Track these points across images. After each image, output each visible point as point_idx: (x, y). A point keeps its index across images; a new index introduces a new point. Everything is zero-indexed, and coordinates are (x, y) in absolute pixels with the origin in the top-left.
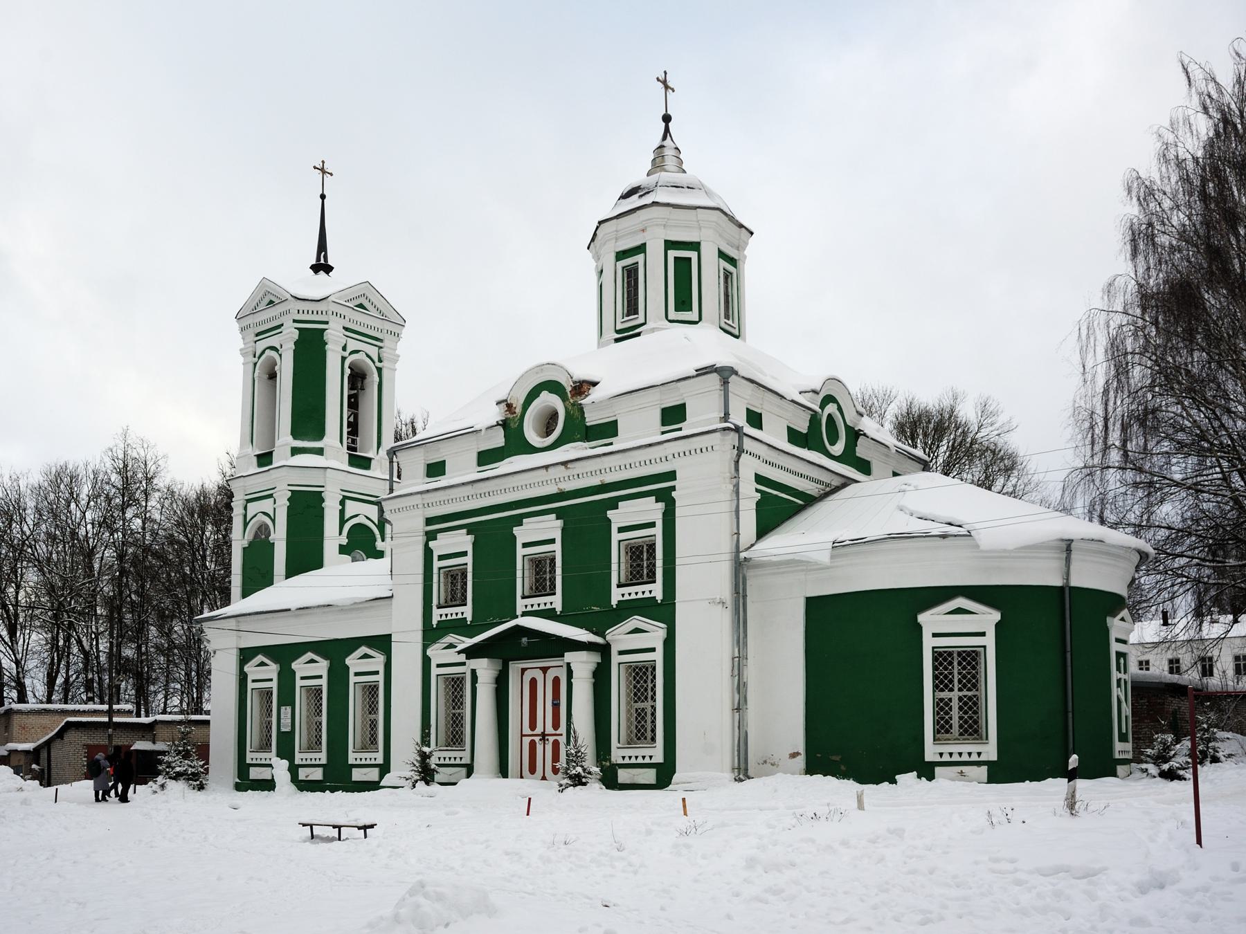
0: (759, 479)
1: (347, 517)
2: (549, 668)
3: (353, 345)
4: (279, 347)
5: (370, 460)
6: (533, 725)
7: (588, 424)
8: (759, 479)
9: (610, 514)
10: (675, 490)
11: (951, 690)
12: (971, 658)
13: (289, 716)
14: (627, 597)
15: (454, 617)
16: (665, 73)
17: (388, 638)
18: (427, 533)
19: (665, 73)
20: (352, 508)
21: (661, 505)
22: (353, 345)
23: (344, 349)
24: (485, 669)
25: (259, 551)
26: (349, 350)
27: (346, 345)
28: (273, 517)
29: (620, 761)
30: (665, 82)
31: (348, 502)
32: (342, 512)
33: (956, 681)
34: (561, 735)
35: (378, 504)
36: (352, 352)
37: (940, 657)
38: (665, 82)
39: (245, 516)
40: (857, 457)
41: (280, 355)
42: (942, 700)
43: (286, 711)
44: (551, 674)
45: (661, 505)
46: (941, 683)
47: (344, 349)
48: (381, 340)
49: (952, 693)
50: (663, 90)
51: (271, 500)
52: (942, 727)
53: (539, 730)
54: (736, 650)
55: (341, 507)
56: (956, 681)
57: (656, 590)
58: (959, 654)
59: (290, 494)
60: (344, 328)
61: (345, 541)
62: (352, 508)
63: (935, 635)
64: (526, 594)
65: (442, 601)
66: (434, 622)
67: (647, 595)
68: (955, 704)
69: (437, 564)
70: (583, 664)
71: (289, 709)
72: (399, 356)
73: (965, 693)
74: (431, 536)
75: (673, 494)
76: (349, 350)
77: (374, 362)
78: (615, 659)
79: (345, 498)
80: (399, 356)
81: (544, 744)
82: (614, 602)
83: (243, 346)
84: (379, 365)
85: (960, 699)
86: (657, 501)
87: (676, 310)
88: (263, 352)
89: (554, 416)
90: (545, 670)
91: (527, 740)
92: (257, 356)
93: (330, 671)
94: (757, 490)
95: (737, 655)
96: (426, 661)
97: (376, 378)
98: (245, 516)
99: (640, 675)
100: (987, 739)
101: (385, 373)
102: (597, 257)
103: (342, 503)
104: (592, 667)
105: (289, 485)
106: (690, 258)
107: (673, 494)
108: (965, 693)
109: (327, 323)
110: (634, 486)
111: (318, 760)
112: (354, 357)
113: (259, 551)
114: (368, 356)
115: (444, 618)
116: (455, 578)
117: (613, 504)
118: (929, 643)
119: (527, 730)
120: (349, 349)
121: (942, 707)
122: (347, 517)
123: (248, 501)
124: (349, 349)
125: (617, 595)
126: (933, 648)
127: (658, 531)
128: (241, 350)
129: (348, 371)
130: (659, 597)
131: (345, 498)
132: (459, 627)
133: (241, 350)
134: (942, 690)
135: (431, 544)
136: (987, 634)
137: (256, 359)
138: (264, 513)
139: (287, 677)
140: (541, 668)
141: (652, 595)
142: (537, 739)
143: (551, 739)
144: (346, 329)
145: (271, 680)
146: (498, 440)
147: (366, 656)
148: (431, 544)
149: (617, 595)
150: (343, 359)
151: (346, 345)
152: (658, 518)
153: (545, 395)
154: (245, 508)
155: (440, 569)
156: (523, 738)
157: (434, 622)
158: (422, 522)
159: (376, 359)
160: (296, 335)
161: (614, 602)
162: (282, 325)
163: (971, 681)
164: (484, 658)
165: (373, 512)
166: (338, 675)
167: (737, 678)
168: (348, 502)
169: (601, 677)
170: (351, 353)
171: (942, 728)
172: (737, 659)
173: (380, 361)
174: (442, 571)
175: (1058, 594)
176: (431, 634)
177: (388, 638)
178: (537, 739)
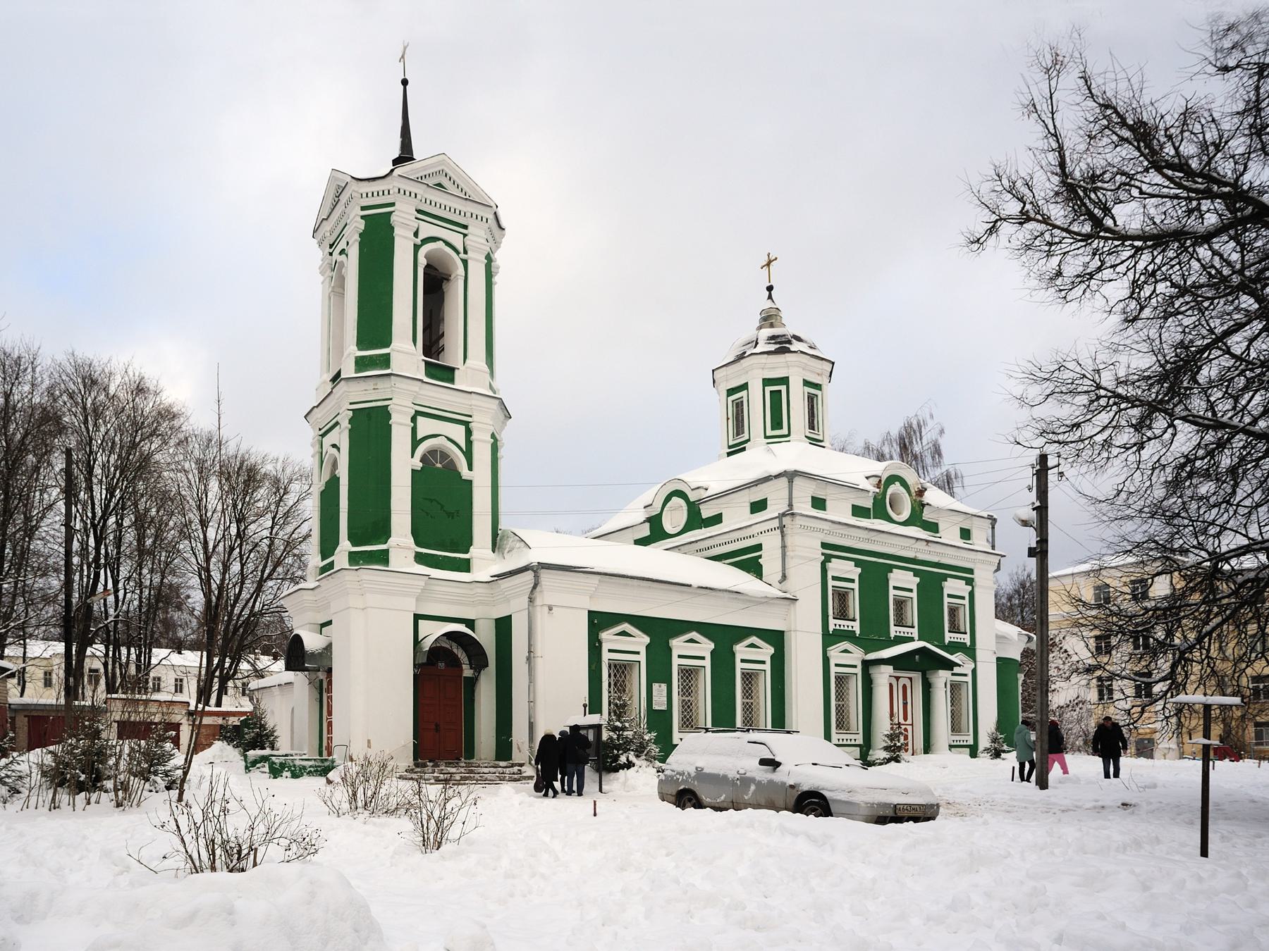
1: (419, 438)
3: (427, 230)
5: (452, 370)
20: (425, 426)
22: (427, 230)
23: (416, 234)
27: (418, 229)
31: (420, 419)
32: (414, 430)
35: (466, 424)
47: (416, 234)
48: (465, 227)
55: (412, 424)
59: (351, 413)
61: (419, 465)
77: (458, 253)
79: (418, 413)
84: (462, 255)
97: (461, 271)
103: (414, 419)
105: (351, 404)
109: (393, 204)
120: (422, 236)
122: (419, 438)
129: (422, 262)
131: (418, 413)
150: (417, 248)
151: (418, 229)
159: (461, 250)
168: (420, 419)
173: (465, 252)
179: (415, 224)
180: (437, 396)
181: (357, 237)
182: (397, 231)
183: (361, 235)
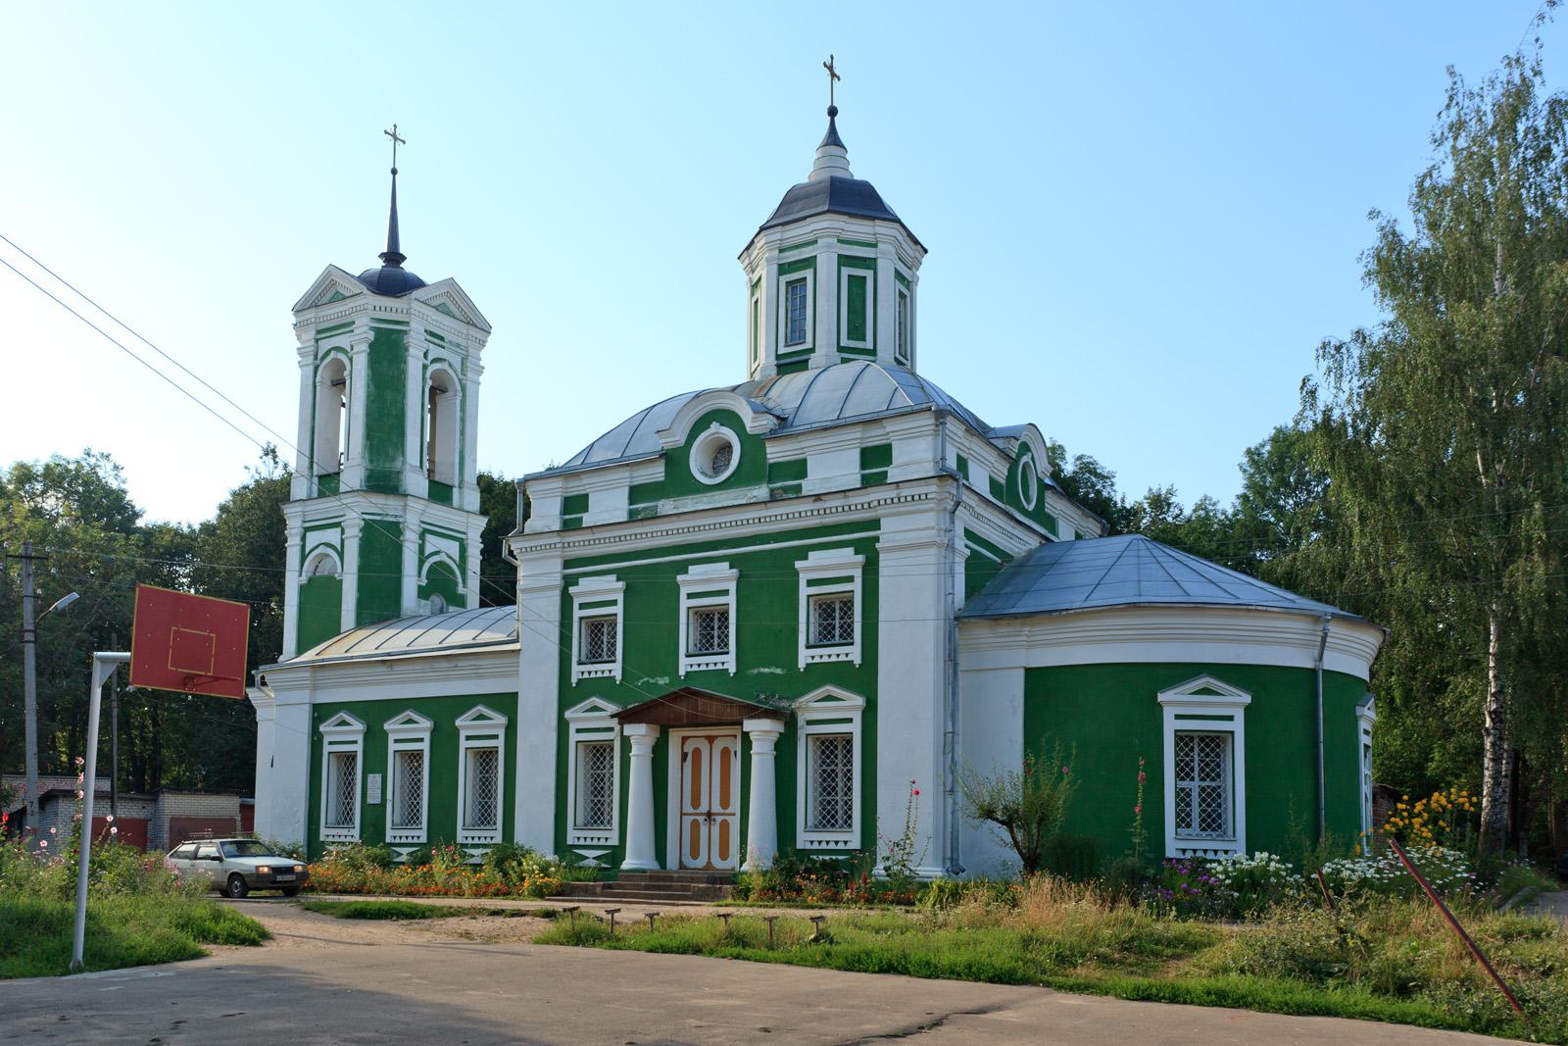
0: (969, 534)
1: (427, 553)
2: (716, 737)
4: (349, 349)
5: (450, 487)
6: (696, 803)
7: (771, 461)
8: (969, 534)
9: (798, 564)
10: (879, 542)
11: (1192, 779)
12: (1214, 743)
13: (379, 785)
14: (817, 660)
15: (599, 675)
16: (832, 57)
17: (513, 697)
18: (565, 577)
19: (832, 57)
20: (433, 543)
21: (861, 558)
23: (426, 355)
24: (640, 735)
25: (321, 593)
26: (430, 358)
28: (339, 548)
29: (808, 846)
30: (831, 68)
31: (429, 537)
32: (422, 548)
33: (1197, 769)
34: (734, 815)
36: (436, 360)
37: (1182, 738)
38: (831, 68)
39: (303, 547)
40: (1046, 513)
41: (351, 360)
42: (1182, 790)
43: (374, 780)
44: (718, 746)
45: (861, 558)
46: (1183, 771)
47: (426, 355)
49: (1192, 783)
50: (829, 78)
51: (339, 529)
52: (1183, 820)
53: (704, 808)
54: (950, 724)
55: (421, 542)
56: (1197, 769)
57: (854, 654)
58: (1202, 739)
60: (426, 331)
61: (424, 582)
62: (433, 543)
63: (1178, 717)
64: (691, 651)
65: (583, 659)
66: (574, 680)
67: (843, 658)
68: (1195, 794)
69: (577, 613)
70: (762, 731)
71: (378, 777)
72: (483, 368)
73: (1207, 783)
74: (569, 581)
75: (877, 545)
76: (430, 358)
78: (803, 730)
80: (483, 368)
81: (710, 824)
82: (802, 665)
83: (299, 345)
85: (1203, 789)
86: (856, 553)
87: (849, 339)
88: (328, 353)
89: (727, 448)
90: (711, 739)
91: (688, 820)
92: (319, 356)
93: (434, 732)
94: (966, 546)
95: (950, 729)
96: (563, 726)
98: (303, 547)
99: (832, 748)
100: (1234, 835)
101: (469, 385)
102: (751, 268)
103: (422, 536)
104: (775, 737)
106: (865, 278)
107: (877, 545)
108: (1207, 783)
110: (826, 534)
111: (416, 838)
112: (438, 366)
113: (321, 593)
114: (450, 365)
115: (586, 676)
116: (597, 628)
117: (802, 553)
118: (1170, 727)
119: (687, 808)
120: (431, 357)
121: (1183, 797)
122: (427, 553)
123: (307, 530)
124: (431, 357)
125: (804, 657)
126: (1176, 731)
127: (857, 587)
128: (298, 349)
130: (858, 661)
132: (603, 687)
133: (298, 349)
134: (1182, 779)
135: (572, 590)
136: (1235, 718)
137: (318, 361)
138: (328, 545)
139: (375, 739)
140: (706, 737)
141: (849, 659)
142: (701, 819)
143: (719, 819)
144: (432, 334)
145: (355, 742)
146: (657, 473)
147: (481, 717)
148: (572, 590)
149: (804, 657)
150: (425, 367)
152: (858, 573)
153: (715, 427)
154: (303, 539)
155: (581, 619)
156: (684, 817)
157: (574, 680)
158: (558, 565)
160: (371, 336)
161: (802, 665)
162: (354, 323)
163: (1213, 769)
164: (640, 722)
165: (453, 548)
166: (444, 739)
167: (950, 755)
168: (429, 537)
169: (785, 750)
170: (432, 362)
171: (1183, 820)
172: (951, 735)
174: (583, 621)
175: (1312, 673)
176: (569, 694)
177: (513, 697)
178: (701, 819)
179: (426, 345)
180: (439, 514)
181: (365, 347)
182: (411, 350)
183: (371, 346)
